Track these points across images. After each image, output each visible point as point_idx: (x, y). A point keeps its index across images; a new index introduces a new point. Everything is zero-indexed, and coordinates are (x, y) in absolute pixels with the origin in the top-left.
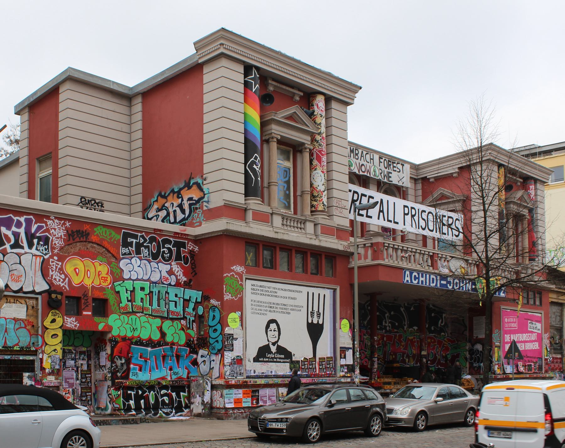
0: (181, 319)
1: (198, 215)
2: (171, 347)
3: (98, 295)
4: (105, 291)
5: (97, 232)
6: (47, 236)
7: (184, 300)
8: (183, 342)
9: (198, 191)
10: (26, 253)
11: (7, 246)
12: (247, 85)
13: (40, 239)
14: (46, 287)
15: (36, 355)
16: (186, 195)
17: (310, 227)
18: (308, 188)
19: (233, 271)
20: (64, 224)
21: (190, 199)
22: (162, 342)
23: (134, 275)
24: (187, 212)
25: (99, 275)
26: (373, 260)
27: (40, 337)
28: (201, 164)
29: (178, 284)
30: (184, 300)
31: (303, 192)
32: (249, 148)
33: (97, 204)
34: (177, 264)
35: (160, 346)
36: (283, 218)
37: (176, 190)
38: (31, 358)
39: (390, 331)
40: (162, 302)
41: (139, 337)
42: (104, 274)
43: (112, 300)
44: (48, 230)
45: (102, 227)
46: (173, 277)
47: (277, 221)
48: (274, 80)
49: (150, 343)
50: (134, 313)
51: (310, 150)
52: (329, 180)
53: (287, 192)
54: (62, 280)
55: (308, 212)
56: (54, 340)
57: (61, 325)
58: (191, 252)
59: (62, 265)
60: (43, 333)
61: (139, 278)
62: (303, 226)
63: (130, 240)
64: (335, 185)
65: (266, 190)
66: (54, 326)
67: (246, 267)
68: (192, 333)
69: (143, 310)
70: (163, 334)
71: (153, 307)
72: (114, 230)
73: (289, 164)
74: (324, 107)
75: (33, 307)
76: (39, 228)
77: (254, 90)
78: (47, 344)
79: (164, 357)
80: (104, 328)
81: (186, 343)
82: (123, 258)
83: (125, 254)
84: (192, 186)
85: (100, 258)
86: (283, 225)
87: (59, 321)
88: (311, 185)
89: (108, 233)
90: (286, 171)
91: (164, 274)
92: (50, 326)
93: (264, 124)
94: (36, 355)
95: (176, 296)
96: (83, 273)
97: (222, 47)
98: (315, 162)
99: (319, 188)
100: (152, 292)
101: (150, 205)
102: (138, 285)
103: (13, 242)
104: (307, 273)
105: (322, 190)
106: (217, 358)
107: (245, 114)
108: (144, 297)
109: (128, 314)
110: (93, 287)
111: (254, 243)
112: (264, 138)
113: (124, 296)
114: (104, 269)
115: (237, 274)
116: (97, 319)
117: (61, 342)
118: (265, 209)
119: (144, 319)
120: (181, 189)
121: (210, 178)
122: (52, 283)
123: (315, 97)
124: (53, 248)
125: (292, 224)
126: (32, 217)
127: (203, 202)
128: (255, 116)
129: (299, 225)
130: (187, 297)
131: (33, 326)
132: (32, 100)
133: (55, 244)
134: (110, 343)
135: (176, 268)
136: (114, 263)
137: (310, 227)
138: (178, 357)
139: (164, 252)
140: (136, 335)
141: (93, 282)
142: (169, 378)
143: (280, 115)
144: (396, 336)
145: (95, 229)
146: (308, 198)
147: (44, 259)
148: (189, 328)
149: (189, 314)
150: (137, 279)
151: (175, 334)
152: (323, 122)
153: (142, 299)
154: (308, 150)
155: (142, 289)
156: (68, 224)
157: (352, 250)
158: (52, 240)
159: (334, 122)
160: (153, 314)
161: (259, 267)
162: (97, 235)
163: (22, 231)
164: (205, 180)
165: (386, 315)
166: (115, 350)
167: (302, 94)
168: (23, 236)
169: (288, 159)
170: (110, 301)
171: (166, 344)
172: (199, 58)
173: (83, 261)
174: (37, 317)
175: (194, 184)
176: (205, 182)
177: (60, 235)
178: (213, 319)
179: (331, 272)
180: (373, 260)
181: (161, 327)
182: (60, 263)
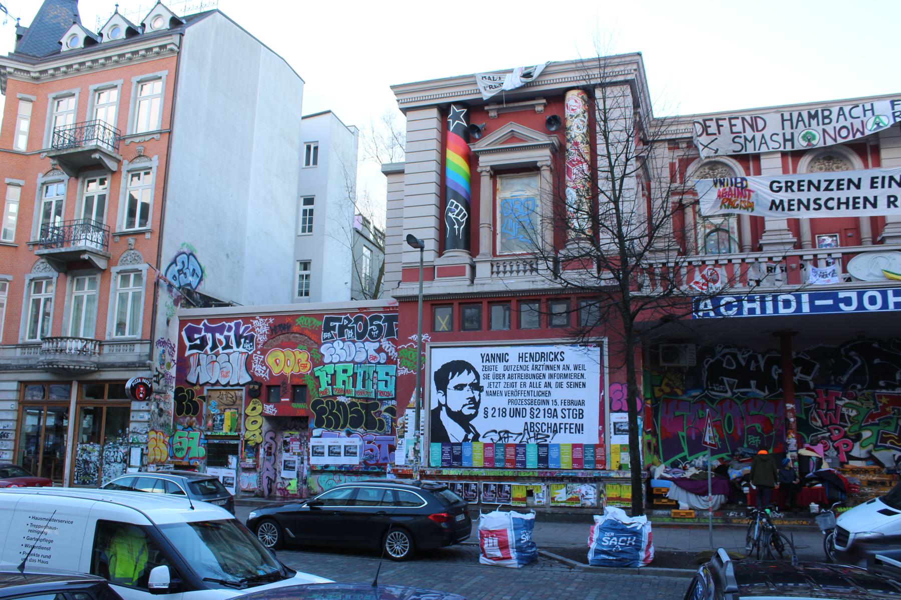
0: (392, 399)
3: (297, 382)
11: (220, 348)
13: (246, 338)
14: (249, 379)
19: (412, 341)
34: (388, 340)
38: (236, 442)
40: (369, 383)
43: (311, 385)
44: (253, 330)
63: (332, 324)
66: (255, 413)
71: (357, 389)
76: (247, 328)
83: (327, 339)
85: (300, 346)
87: (259, 408)
95: (387, 374)
96: (285, 362)
102: (340, 368)
103: (224, 344)
114: (303, 356)
124: (257, 344)
135: (386, 344)
150: (340, 362)
155: (345, 371)
163: (232, 334)
168: (233, 338)
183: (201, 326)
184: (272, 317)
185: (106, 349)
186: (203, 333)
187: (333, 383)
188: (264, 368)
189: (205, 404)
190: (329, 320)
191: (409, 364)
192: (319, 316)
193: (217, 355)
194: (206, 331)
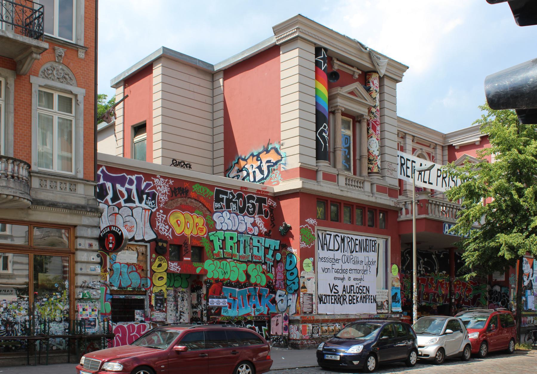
0: (263, 264)
1: (276, 176)
2: (255, 288)
3: (196, 243)
4: (202, 240)
5: (195, 189)
6: (154, 192)
7: (265, 248)
8: (264, 284)
9: (276, 154)
10: (137, 207)
11: (122, 201)
12: (318, 64)
13: (148, 195)
14: (154, 236)
15: (145, 295)
16: (265, 158)
17: (367, 186)
18: (366, 154)
19: (307, 223)
20: (168, 182)
21: (269, 162)
22: (247, 283)
23: (225, 226)
24: (266, 173)
25: (197, 226)
26: (419, 214)
27: (149, 280)
28: (278, 131)
29: (260, 234)
30: (265, 248)
31: (361, 157)
32: (320, 118)
33: (186, 165)
34: (259, 217)
35: (246, 287)
36: (346, 179)
37: (255, 154)
38: (142, 297)
39: (424, 275)
40: (248, 249)
41: (229, 279)
42: (200, 226)
44: (154, 188)
45: (199, 185)
46: (256, 228)
47: (342, 180)
48: (338, 60)
49: (238, 284)
50: (225, 259)
51: (368, 120)
52: (382, 146)
53: (348, 156)
54: (166, 230)
55: (365, 172)
56: (160, 282)
57: (166, 269)
58: (271, 207)
59: (166, 218)
60: (152, 275)
61: (229, 228)
62: (362, 185)
63: (221, 196)
64: (387, 150)
65: (332, 155)
67: (318, 219)
68: (271, 276)
69: (232, 256)
70: (248, 276)
71: (241, 254)
72: (209, 188)
73: (349, 133)
74: (378, 84)
75: (143, 254)
76: (148, 185)
77: (323, 68)
78: (154, 285)
79: (249, 297)
80: (200, 272)
81: (267, 284)
82: (216, 212)
83: (217, 208)
84: (270, 151)
85: (197, 211)
86: (346, 184)
87: (165, 265)
88: (368, 150)
89: (204, 190)
90: (347, 139)
91: (249, 226)
92: (157, 270)
93: (331, 98)
94: (145, 295)
96: (184, 224)
97: (297, 31)
98: (371, 131)
99: (374, 153)
100: (239, 241)
101: (232, 167)
102: (228, 234)
104: (365, 225)
105: (377, 155)
106: (294, 298)
107: (316, 89)
108: (233, 245)
109: (220, 259)
110: (191, 236)
111: (324, 200)
112: (330, 110)
113: (217, 244)
114: (200, 221)
115: (311, 225)
116: (195, 264)
117: (166, 284)
118: (333, 171)
119: (232, 264)
120: (260, 153)
121: (287, 143)
122: (159, 233)
123: (371, 75)
124: (159, 203)
125: (353, 184)
126: (141, 176)
127: (280, 164)
128: (323, 90)
129: (359, 185)
130: (267, 246)
131: (143, 270)
132: (127, 75)
133: (161, 199)
134: (206, 284)
135: (259, 221)
136: (208, 216)
137: (367, 186)
138: (260, 296)
139: (248, 206)
140: (226, 278)
141: (191, 232)
142: (253, 315)
143: (344, 90)
144: (428, 278)
145: (193, 187)
146: (365, 161)
147: (152, 212)
148: (269, 272)
149: (269, 259)
150: (227, 230)
151: (258, 276)
152: (378, 96)
153: (231, 247)
154: (366, 121)
155: (232, 238)
156: (171, 182)
157: (401, 206)
158: (158, 196)
159: (386, 97)
160: (240, 260)
161: (327, 220)
162: (195, 192)
163: (134, 188)
164: (282, 145)
165: (421, 261)
166: (210, 290)
167: (360, 72)
168: (134, 192)
169: (349, 128)
170: (206, 248)
171: (251, 285)
172: (277, 40)
173: (183, 214)
174: (146, 262)
175: (272, 148)
176: (282, 147)
177: (164, 191)
178: (290, 264)
179: (383, 224)
180: (419, 214)
181: (247, 270)
182: (165, 216)
183: (99, 172)
184: (172, 179)
185: (35, 183)
186: (102, 181)
187: (223, 248)
188: (167, 227)
189: (108, 257)
190: (218, 192)
191: (306, 240)
192: (211, 187)
193: (119, 207)
194: (104, 180)
